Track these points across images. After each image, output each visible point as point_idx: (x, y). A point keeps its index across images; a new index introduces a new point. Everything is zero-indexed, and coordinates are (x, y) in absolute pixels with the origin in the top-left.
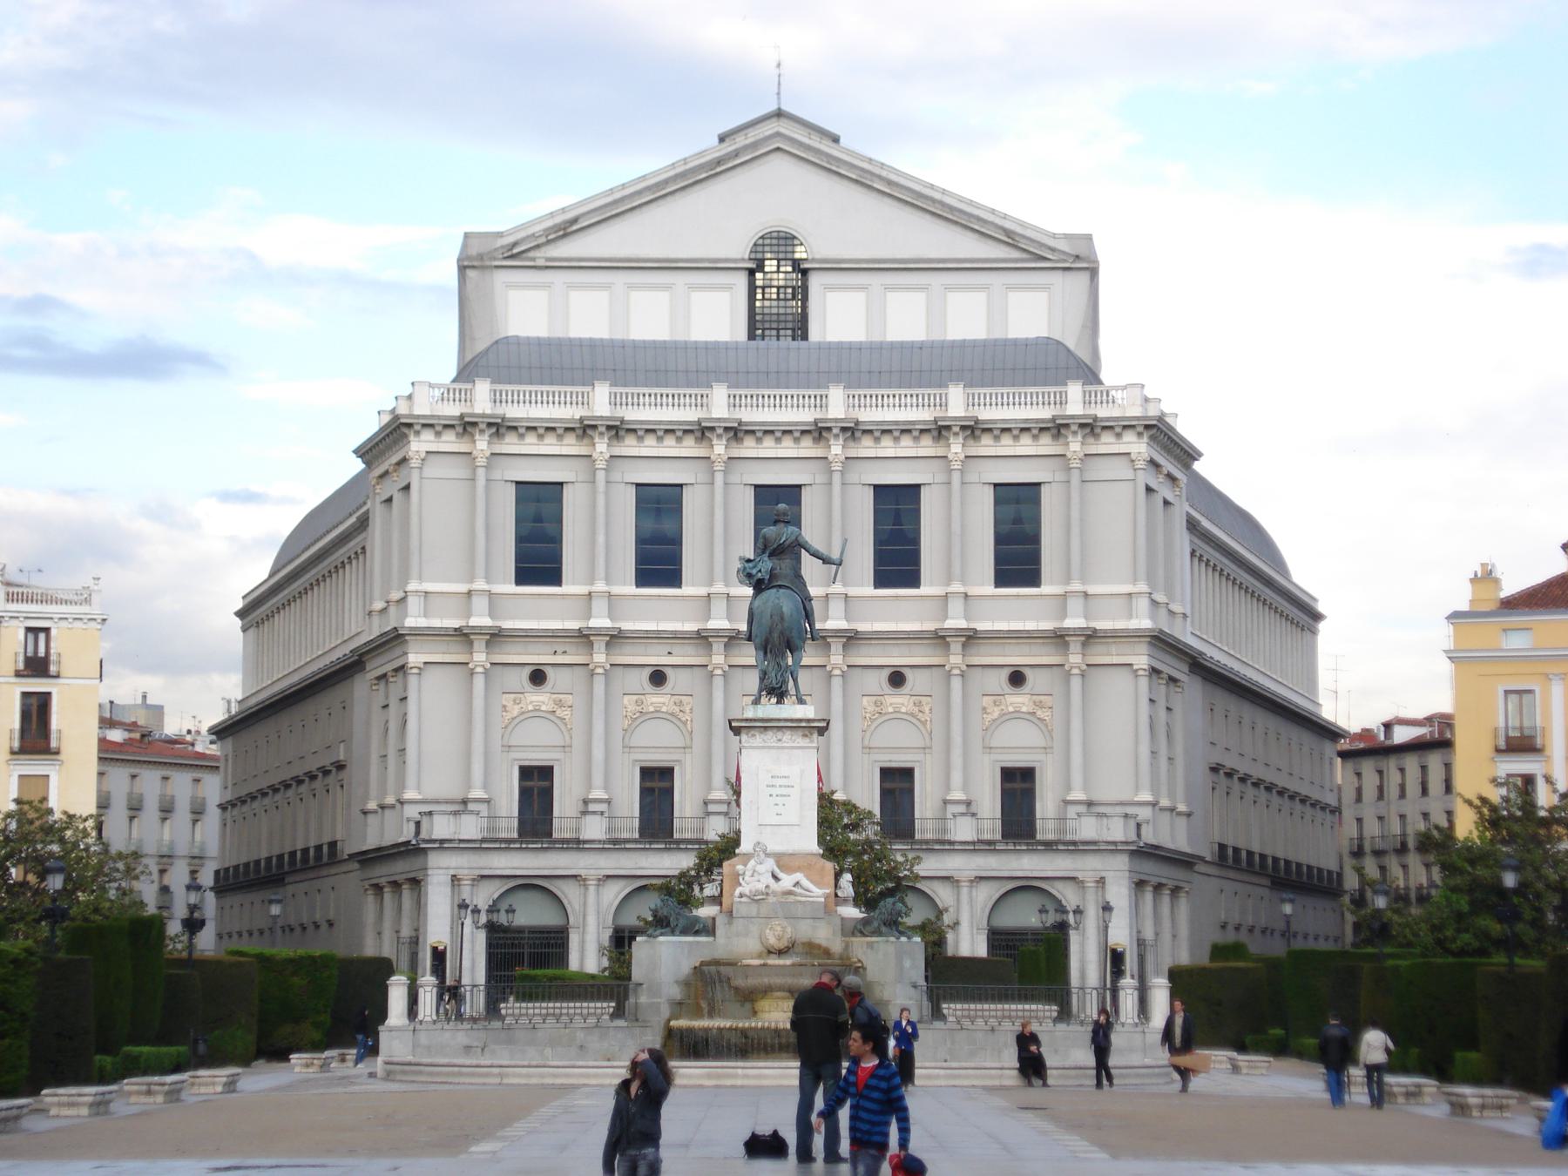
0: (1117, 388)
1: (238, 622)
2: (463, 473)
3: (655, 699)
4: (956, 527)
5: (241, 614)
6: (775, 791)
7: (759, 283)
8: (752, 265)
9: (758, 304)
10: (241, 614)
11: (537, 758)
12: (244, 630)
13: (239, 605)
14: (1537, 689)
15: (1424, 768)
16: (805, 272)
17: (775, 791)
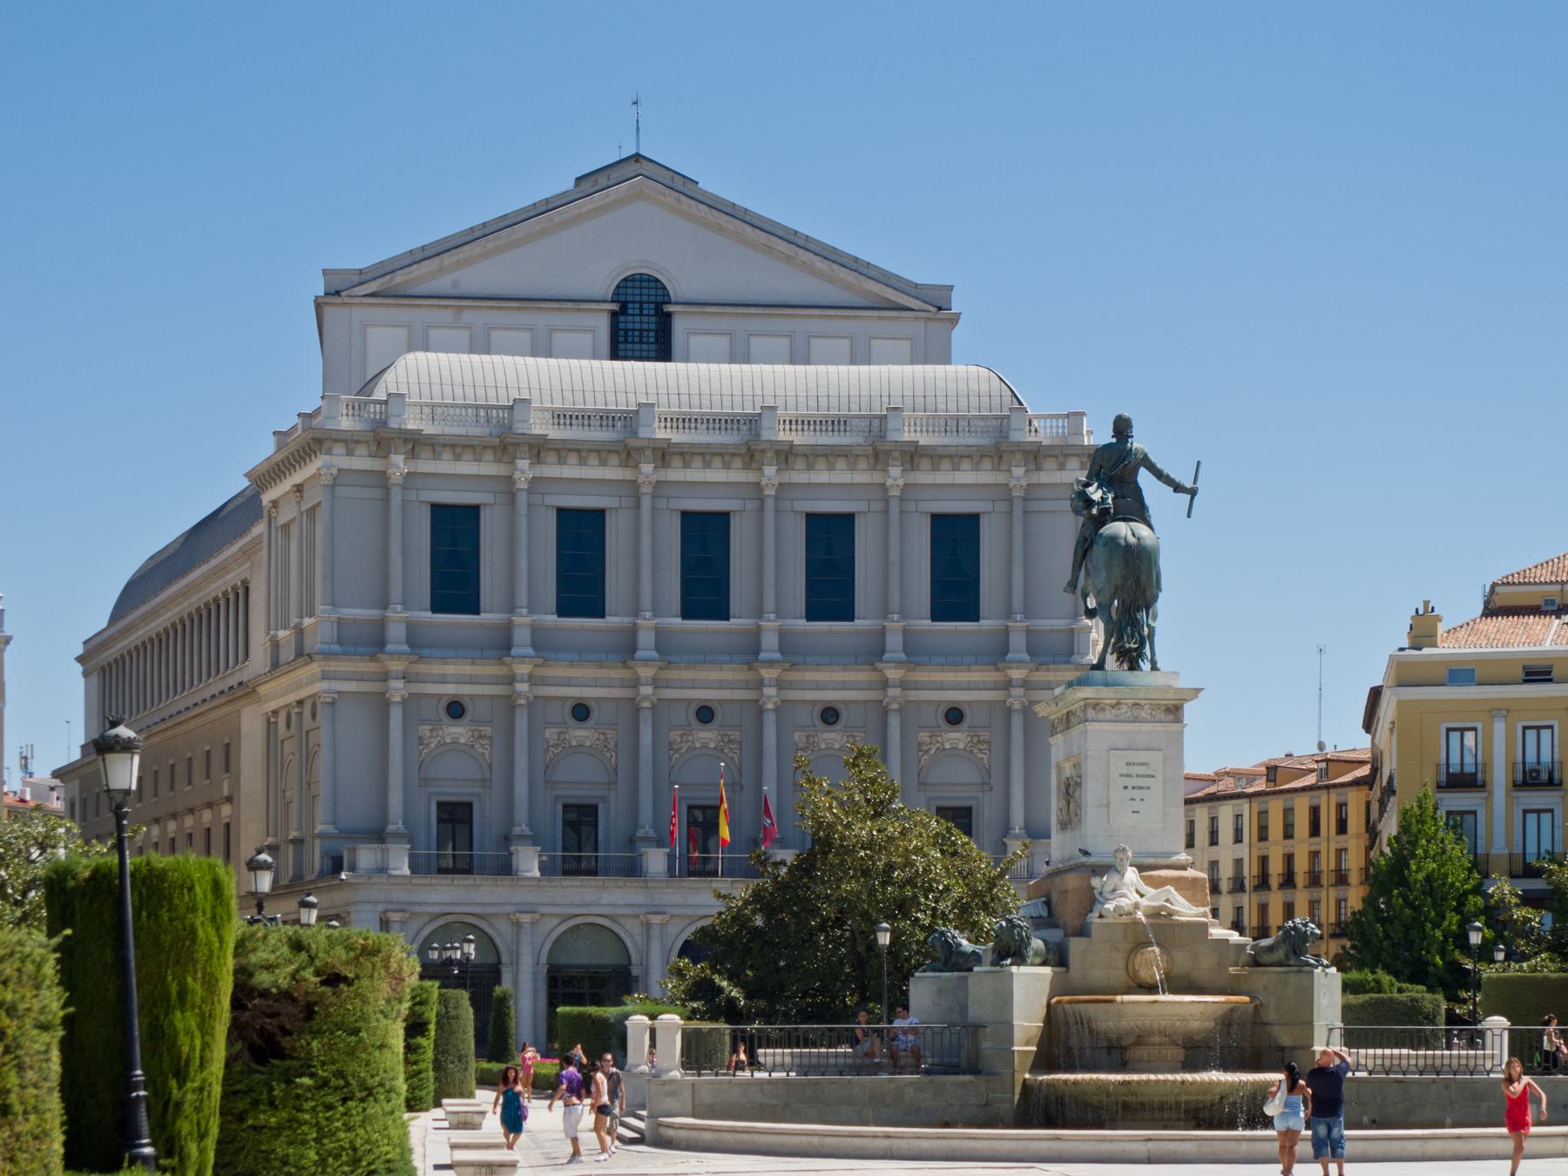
0: (1038, 417)
1: (79, 668)
2: (377, 493)
3: (579, 733)
4: (894, 556)
5: (80, 659)
6: (1130, 782)
7: (622, 326)
8: (615, 307)
9: (621, 346)
10: (80, 659)
11: (455, 793)
12: (86, 674)
13: (80, 651)
14: (1479, 726)
15: (1213, 820)
16: (669, 315)
17: (1130, 782)
